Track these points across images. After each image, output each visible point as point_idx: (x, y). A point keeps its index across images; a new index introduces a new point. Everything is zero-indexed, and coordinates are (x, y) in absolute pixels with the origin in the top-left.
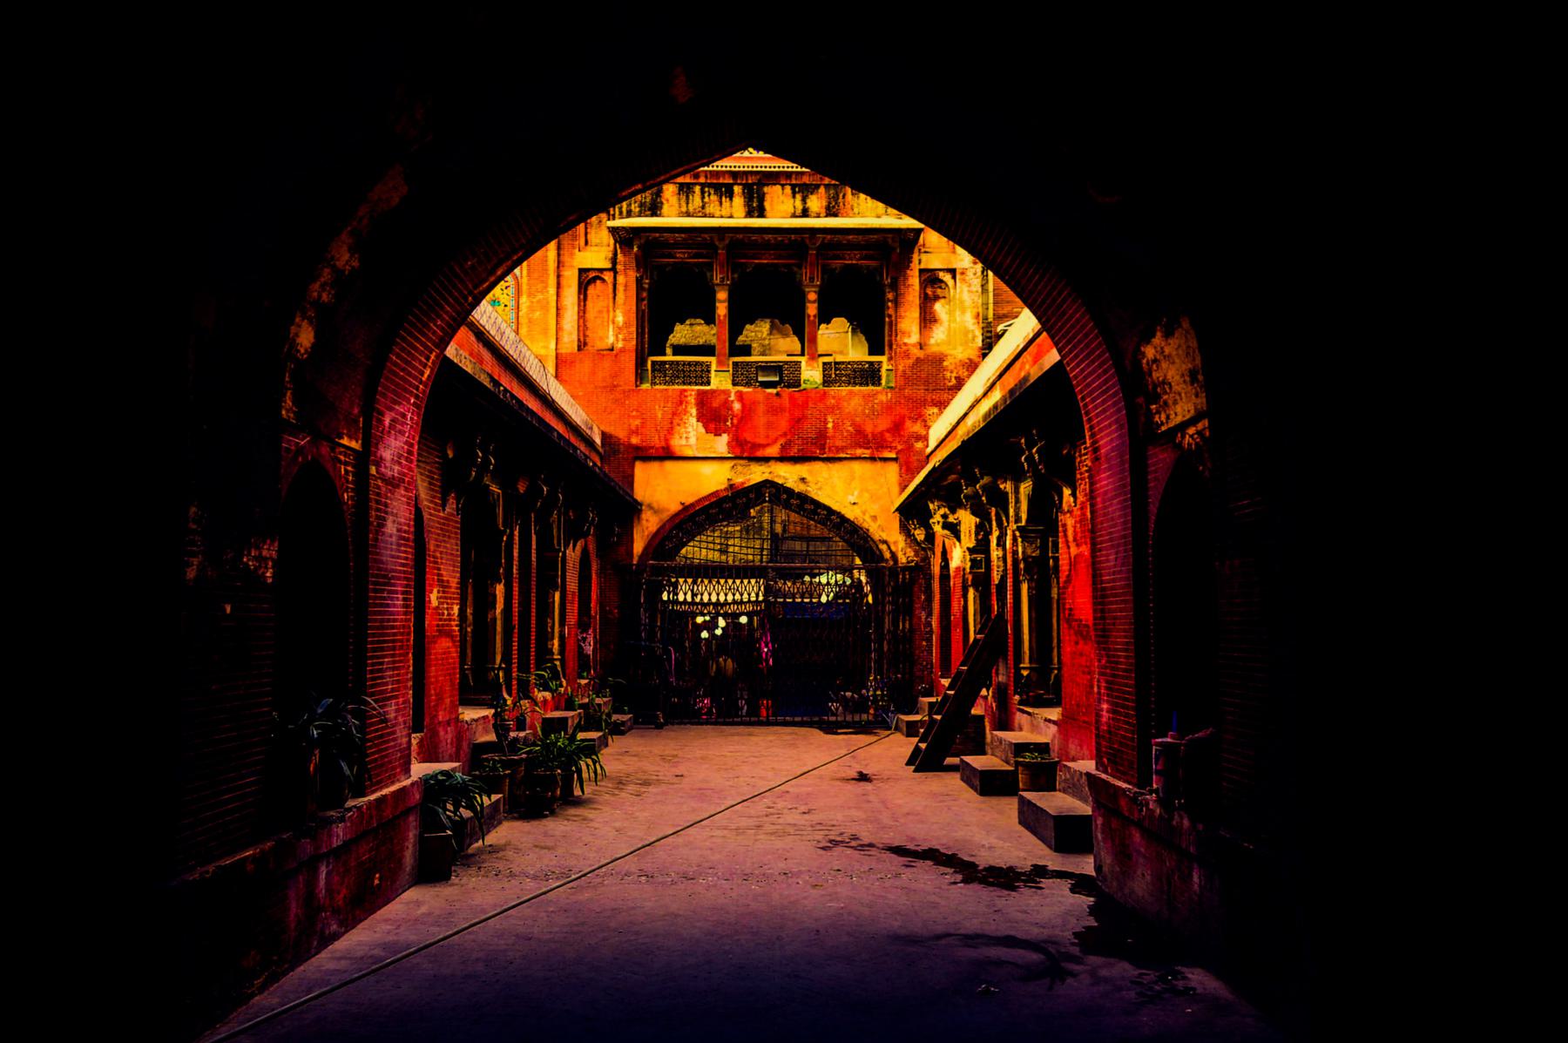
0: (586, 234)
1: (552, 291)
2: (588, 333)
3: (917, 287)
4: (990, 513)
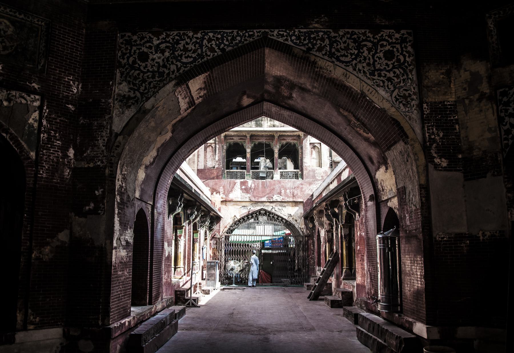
2: (207, 162)
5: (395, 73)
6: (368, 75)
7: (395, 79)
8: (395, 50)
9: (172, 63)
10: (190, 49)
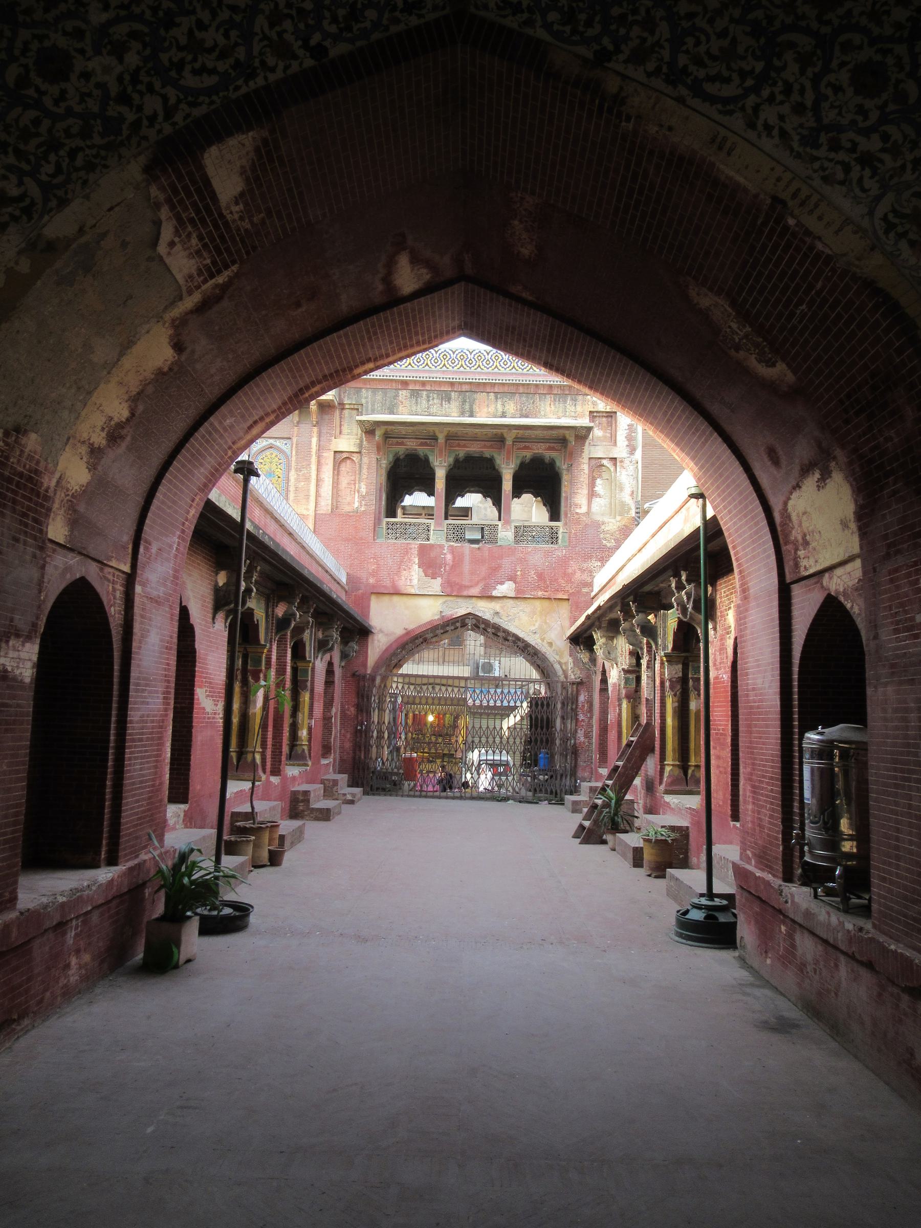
0: (341, 425)
1: (314, 467)
2: (340, 499)
3: (586, 471)
4: (641, 642)
5: (885, 137)
6: (795, 145)
7: (886, 157)
8: (890, 61)
9: (150, 89)
10: (209, 43)
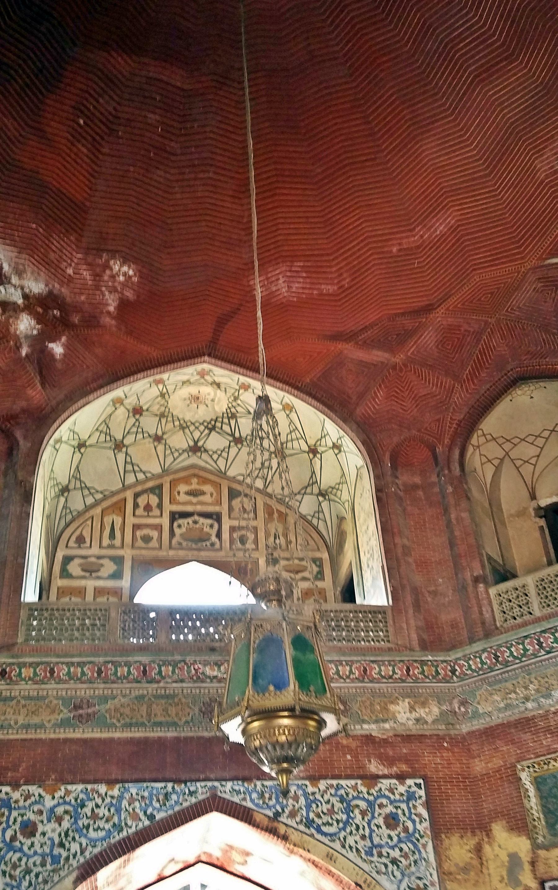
5: (401, 850)
6: (363, 856)
7: (402, 860)
8: (400, 812)
9: (74, 839)
10: (101, 815)
